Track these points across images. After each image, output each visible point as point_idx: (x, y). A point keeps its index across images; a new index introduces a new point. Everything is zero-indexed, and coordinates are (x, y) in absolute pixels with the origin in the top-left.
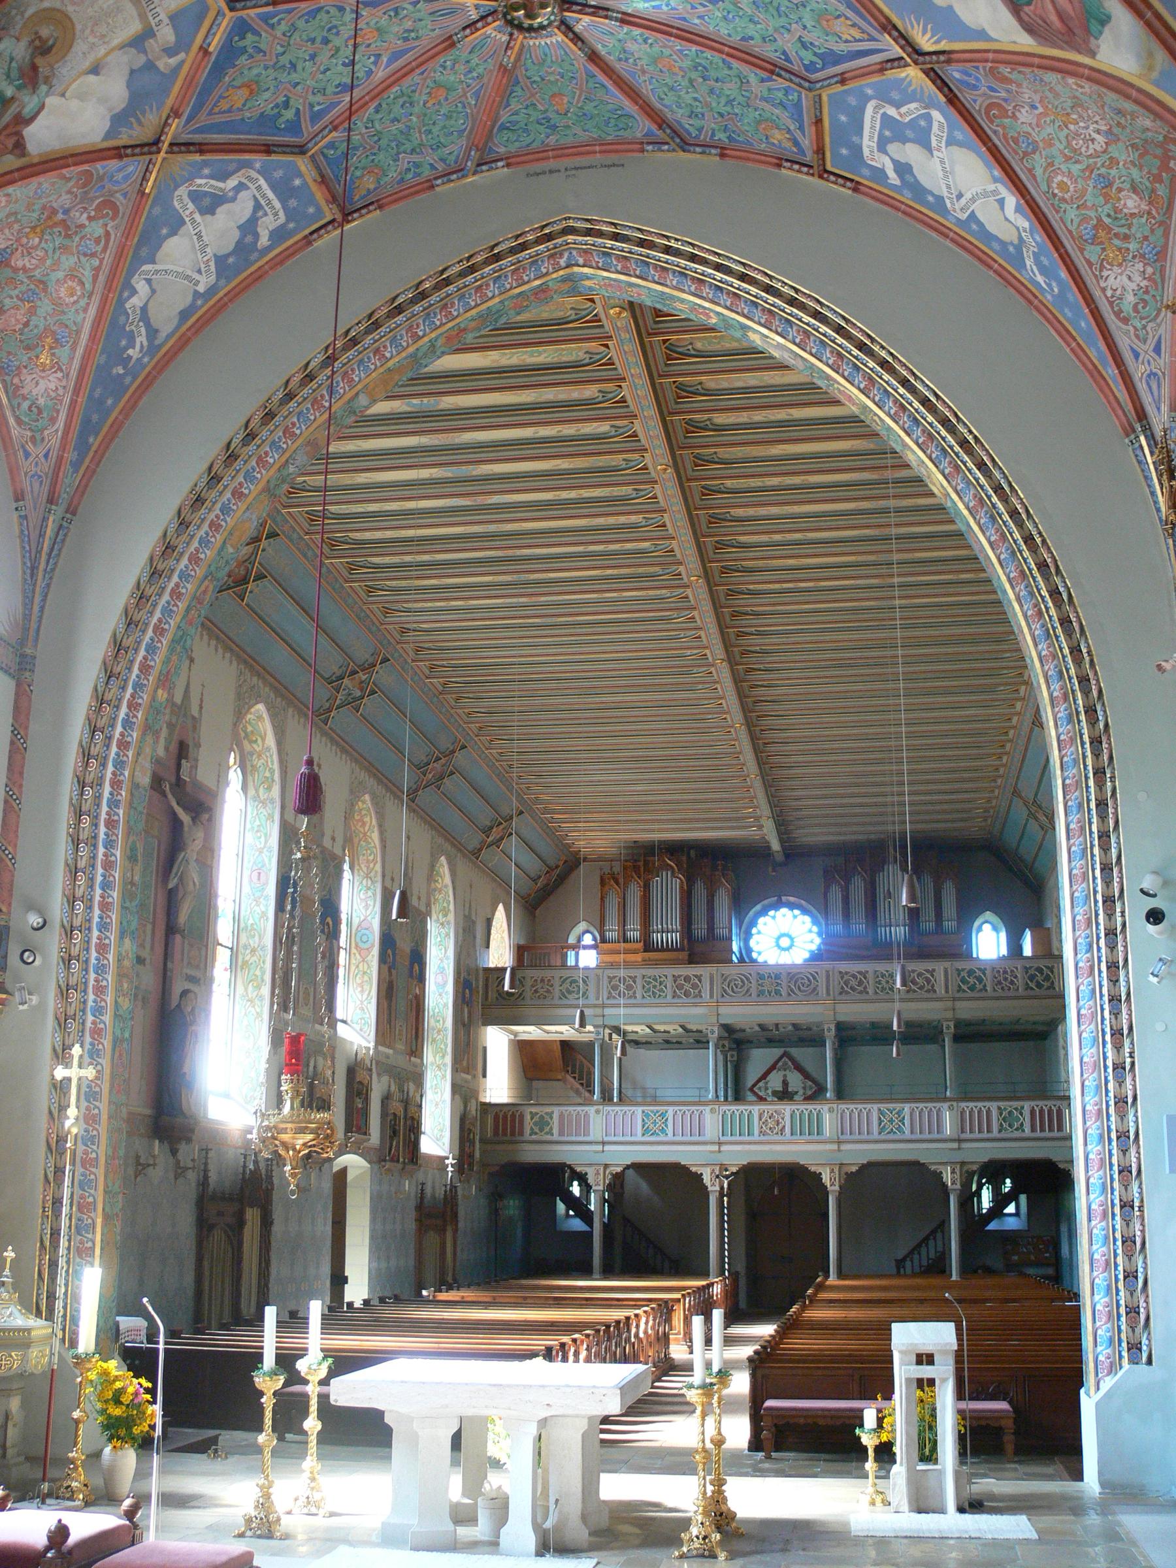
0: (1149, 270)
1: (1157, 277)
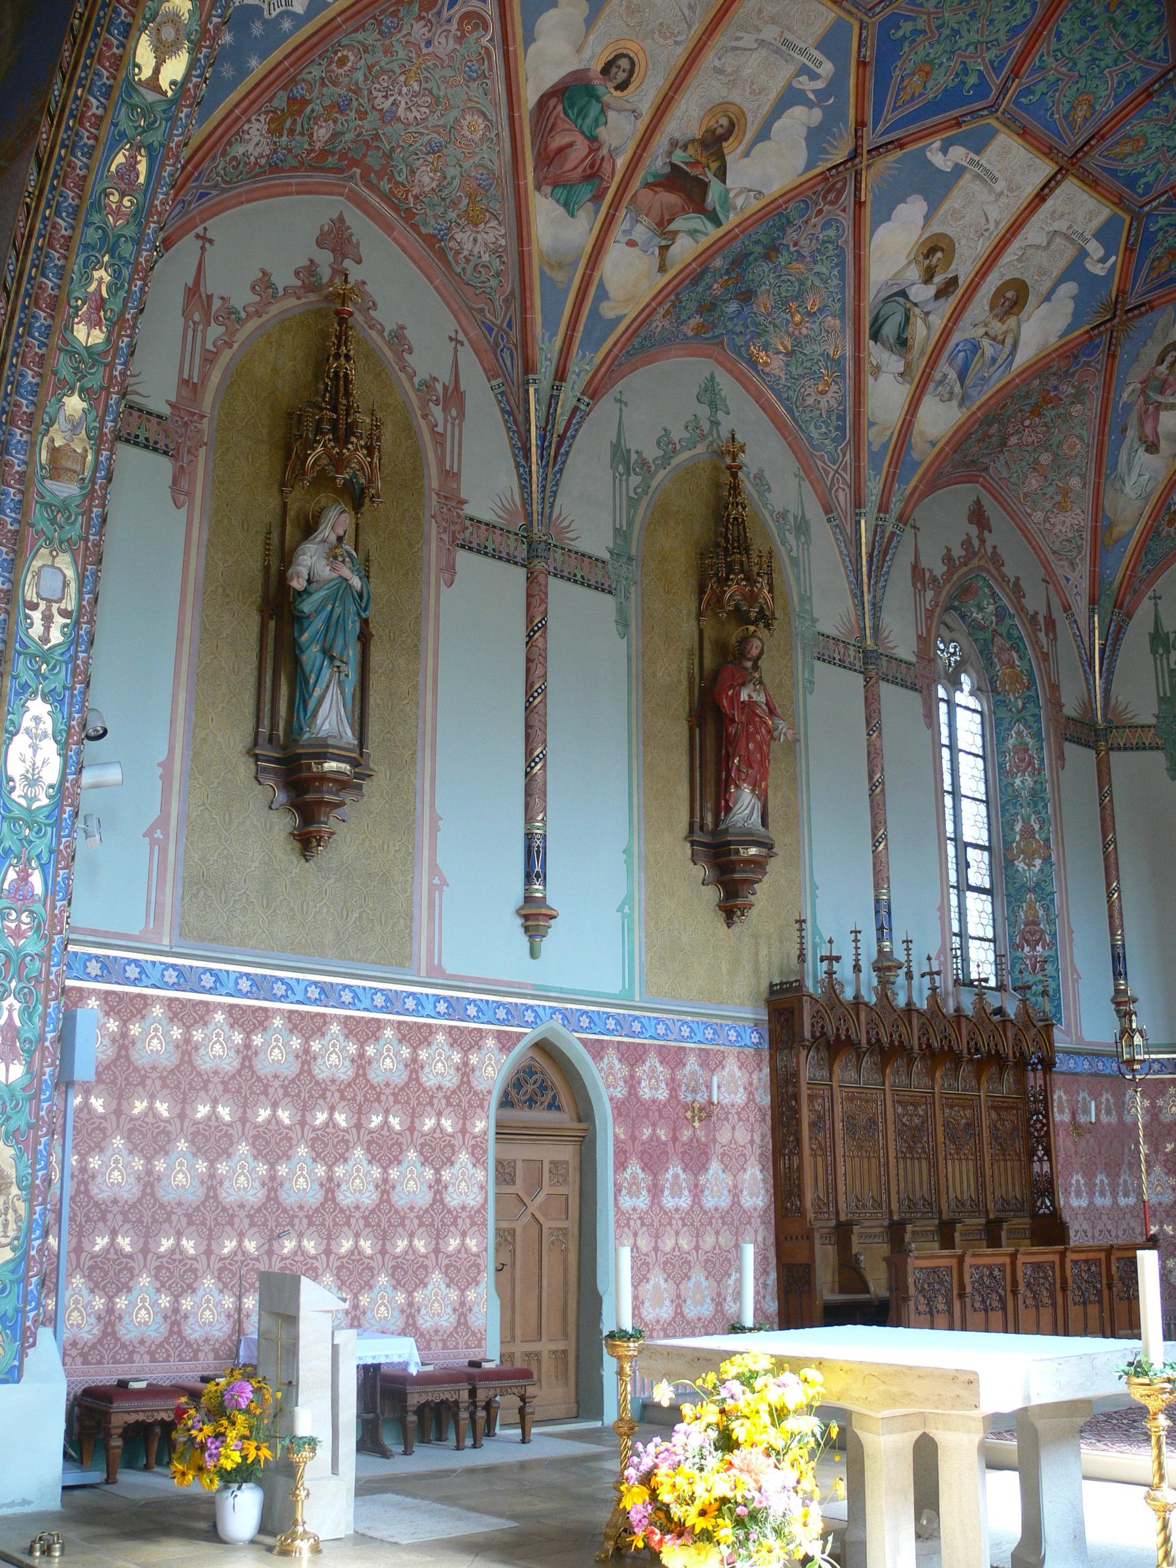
0: (263, 161)
1: (257, 170)
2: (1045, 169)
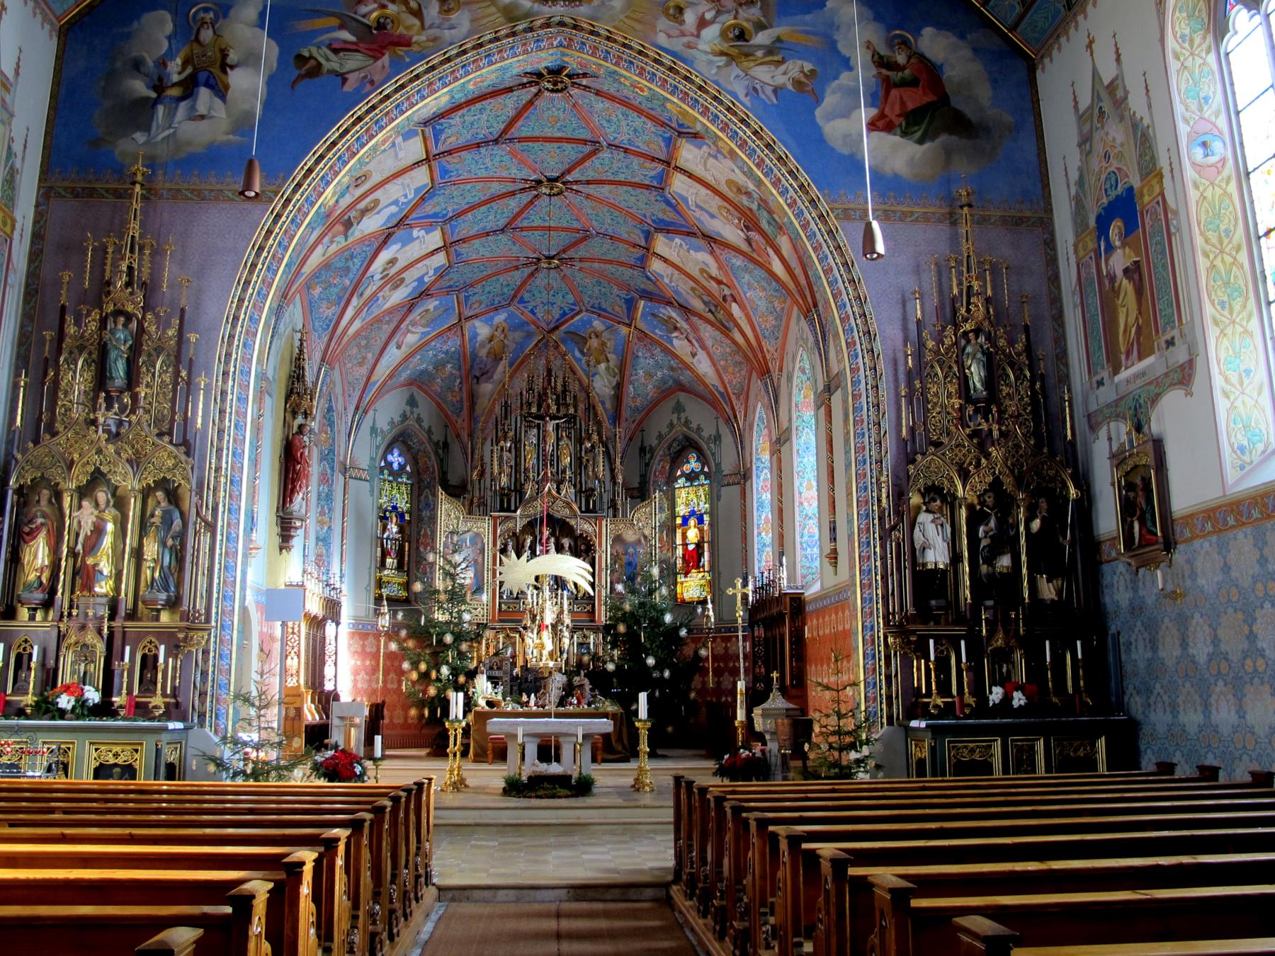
2: (441, 244)
